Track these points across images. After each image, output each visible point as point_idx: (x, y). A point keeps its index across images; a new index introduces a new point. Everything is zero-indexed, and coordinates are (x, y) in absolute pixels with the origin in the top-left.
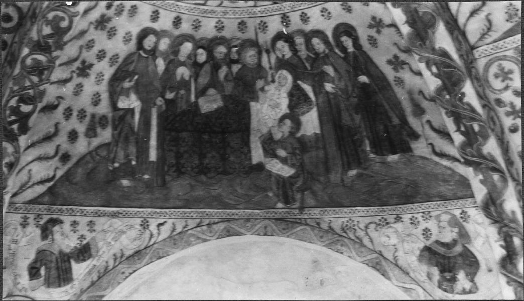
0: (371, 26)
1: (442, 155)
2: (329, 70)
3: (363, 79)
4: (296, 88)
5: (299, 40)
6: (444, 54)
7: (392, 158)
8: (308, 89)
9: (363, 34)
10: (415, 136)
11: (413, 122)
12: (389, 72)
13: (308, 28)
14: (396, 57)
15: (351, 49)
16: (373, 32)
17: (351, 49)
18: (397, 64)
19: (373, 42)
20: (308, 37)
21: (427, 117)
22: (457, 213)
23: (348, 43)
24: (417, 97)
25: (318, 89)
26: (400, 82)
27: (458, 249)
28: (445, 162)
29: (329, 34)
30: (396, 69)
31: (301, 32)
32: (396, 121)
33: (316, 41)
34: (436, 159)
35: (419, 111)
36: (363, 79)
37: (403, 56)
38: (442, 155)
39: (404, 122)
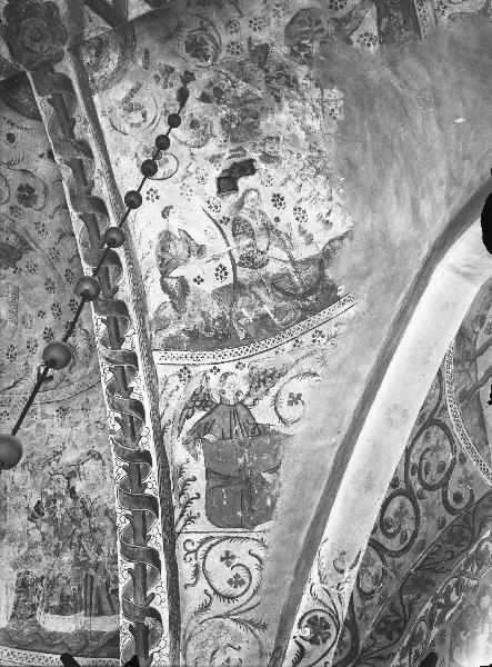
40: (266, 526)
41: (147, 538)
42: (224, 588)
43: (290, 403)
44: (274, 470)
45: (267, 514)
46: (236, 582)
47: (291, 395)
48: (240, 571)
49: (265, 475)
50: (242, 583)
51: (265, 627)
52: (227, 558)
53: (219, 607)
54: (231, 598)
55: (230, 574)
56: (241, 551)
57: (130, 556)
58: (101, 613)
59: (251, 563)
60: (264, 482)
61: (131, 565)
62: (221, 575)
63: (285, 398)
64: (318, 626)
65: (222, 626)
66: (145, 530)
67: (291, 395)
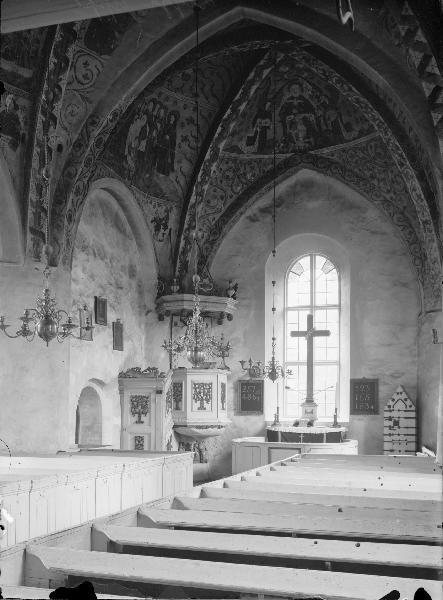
1: (178, 182)
2: (159, 125)
3: (168, 137)
4: (145, 126)
5: (158, 106)
7: (161, 175)
9: (182, 119)
10: (173, 170)
12: (178, 141)
16: (185, 122)
20: (162, 106)
23: (173, 118)
25: (151, 133)
31: (160, 103)
33: (162, 111)
37: (191, 139)
40: (107, 57)
41: (66, 51)
42: (80, 77)
44: (120, 32)
45: (110, 52)
46: (85, 77)
49: (116, 34)
51: (91, 102)
52: (86, 64)
53: (75, 85)
55: (84, 72)
56: (93, 63)
57: (56, 55)
59: (95, 71)
60: (114, 36)
62: (81, 72)
64: (115, 114)
65: (74, 95)
66: (67, 47)
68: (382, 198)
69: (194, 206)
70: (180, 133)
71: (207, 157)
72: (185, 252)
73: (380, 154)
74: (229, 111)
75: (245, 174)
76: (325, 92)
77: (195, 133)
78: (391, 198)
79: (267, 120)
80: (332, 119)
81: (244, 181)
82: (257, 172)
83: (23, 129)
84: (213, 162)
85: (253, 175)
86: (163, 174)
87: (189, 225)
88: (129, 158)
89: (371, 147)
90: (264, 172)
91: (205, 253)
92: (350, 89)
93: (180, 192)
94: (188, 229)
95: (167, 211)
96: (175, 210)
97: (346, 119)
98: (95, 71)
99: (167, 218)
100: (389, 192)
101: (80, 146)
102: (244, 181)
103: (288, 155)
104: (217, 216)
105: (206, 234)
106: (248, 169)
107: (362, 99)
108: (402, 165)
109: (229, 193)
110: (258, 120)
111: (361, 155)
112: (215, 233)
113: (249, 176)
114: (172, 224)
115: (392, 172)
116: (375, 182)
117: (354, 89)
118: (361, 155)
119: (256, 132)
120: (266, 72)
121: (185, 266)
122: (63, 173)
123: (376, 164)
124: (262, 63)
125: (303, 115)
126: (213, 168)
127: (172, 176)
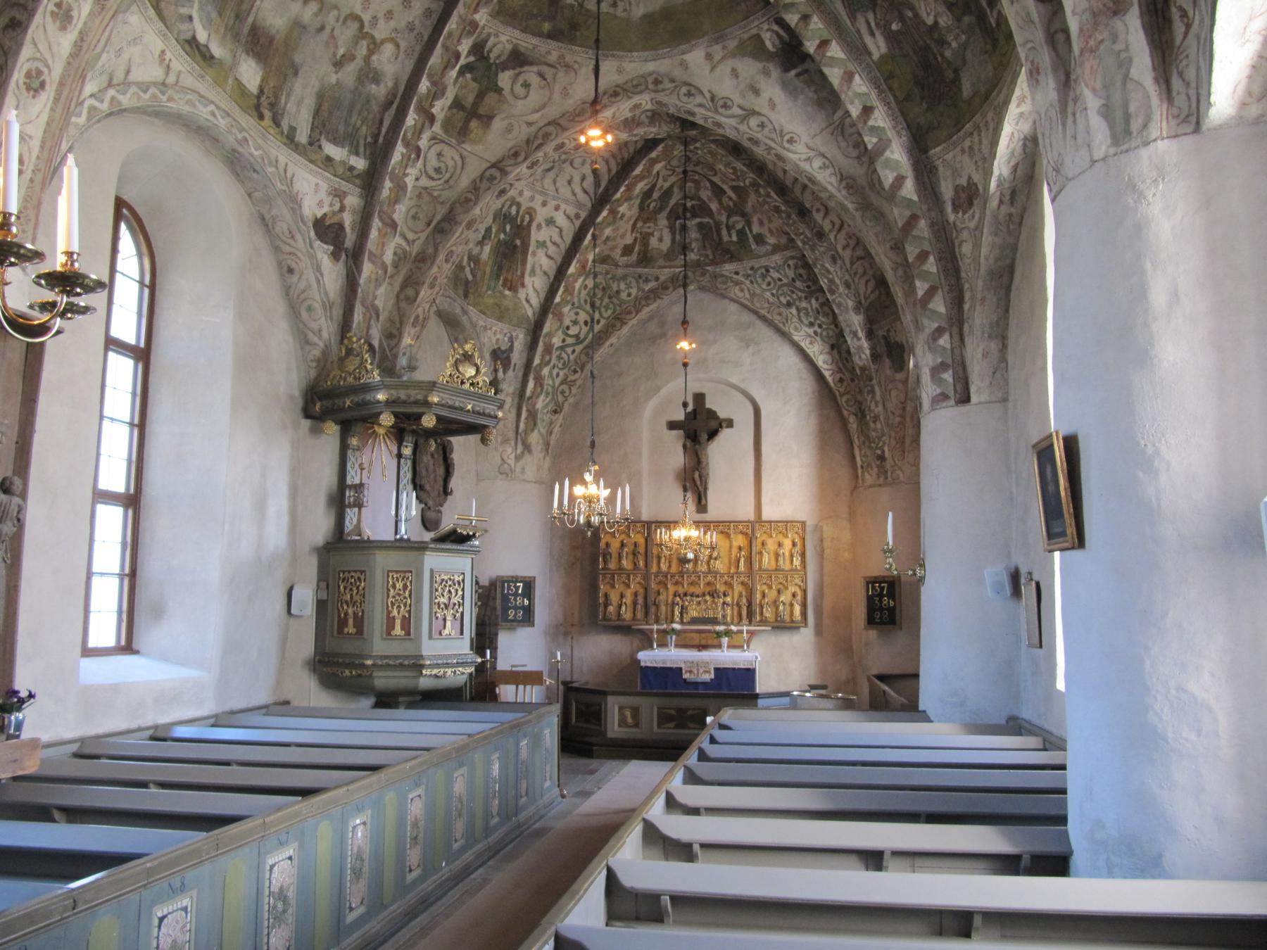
0: (546, 220)
6: (587, 260)
7: (507, 292)
8: (494, 230)
10: (523, 285)
11: (527, 279)
13: (518, 199)
14: (544, 242)
15: (525, 223)
17: (525, 223)
18: (542, 244)
19: (539, 227)
21: (533, 279)
22: (514, 334)
24: (537, 266)
26: (534, 254)
27: (505, 355)
28: (527, 306)
29: (523, 209)
30: (538, 247)
32: (519, 273)
34: (524, 302)
35: (533, 272)
36: (518, 242)
37: (549, 244)
38: (528, 301)
39: (523, 275)
43: (522, 85)
46: (437, 170)
47: (525, 81)
48: (442, 165)
50: (441, 173)
54: (432, 179)
58: (357, 154)
61: (404, 151)
62: (433, 162)
63: (521, 80)
67: (525, 81)
68: (802, 333)
69: (550, 335)
70: (536, 236)
71: (572, 270)
72: (535, 395)
73: (801, 275)
74: (605, 213)
75: (618, 292)
76: (731, 193)
77: (557, 239)
78: (815, 333)
79: (652, 225)
80: (739, 226)
81: (616, 301)
82: (634, 291)
83: (350, 239)
84: (580, 275)
85: (629, 295)
86: (510, 289)
87: (542, 360)
88: (468, 269)
89: (789, 266)
90: (643, 290)
91: (560, 399)
92: (768, 195)
93: (530, 313)
94: (541, 366)
95: (511, 340)
96: (521, 336)
97: (756, 229)
98: (451, 164)
99: (511, 348)
100: (811, 324)
101: (423, 260)
102: (616, 301)
103: (677, 270)
104: (579, 348)
105: (562, 373)
106: (623, 286)
107: (783, 208)
108: (832, 292)
109: (597, 316)
110: (640, 224)
111: (776, 275)
112: (575, 372)
113: (624, 296)
114: (517, 357)
115: (817, 299)
116: (794, 311)
117: (773, 194)
118: (776, 275)
119: (636, 239)
120: (658, 167)
121: (533, 415)
122: (398, 296)
123: (796, 288)
124: (654, 155)
125: (698, 220)
126: (577, 285)
127: (522, 294)
